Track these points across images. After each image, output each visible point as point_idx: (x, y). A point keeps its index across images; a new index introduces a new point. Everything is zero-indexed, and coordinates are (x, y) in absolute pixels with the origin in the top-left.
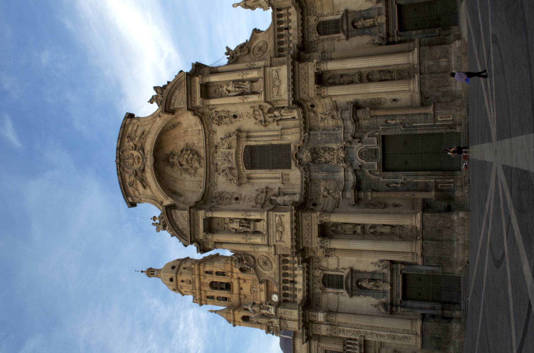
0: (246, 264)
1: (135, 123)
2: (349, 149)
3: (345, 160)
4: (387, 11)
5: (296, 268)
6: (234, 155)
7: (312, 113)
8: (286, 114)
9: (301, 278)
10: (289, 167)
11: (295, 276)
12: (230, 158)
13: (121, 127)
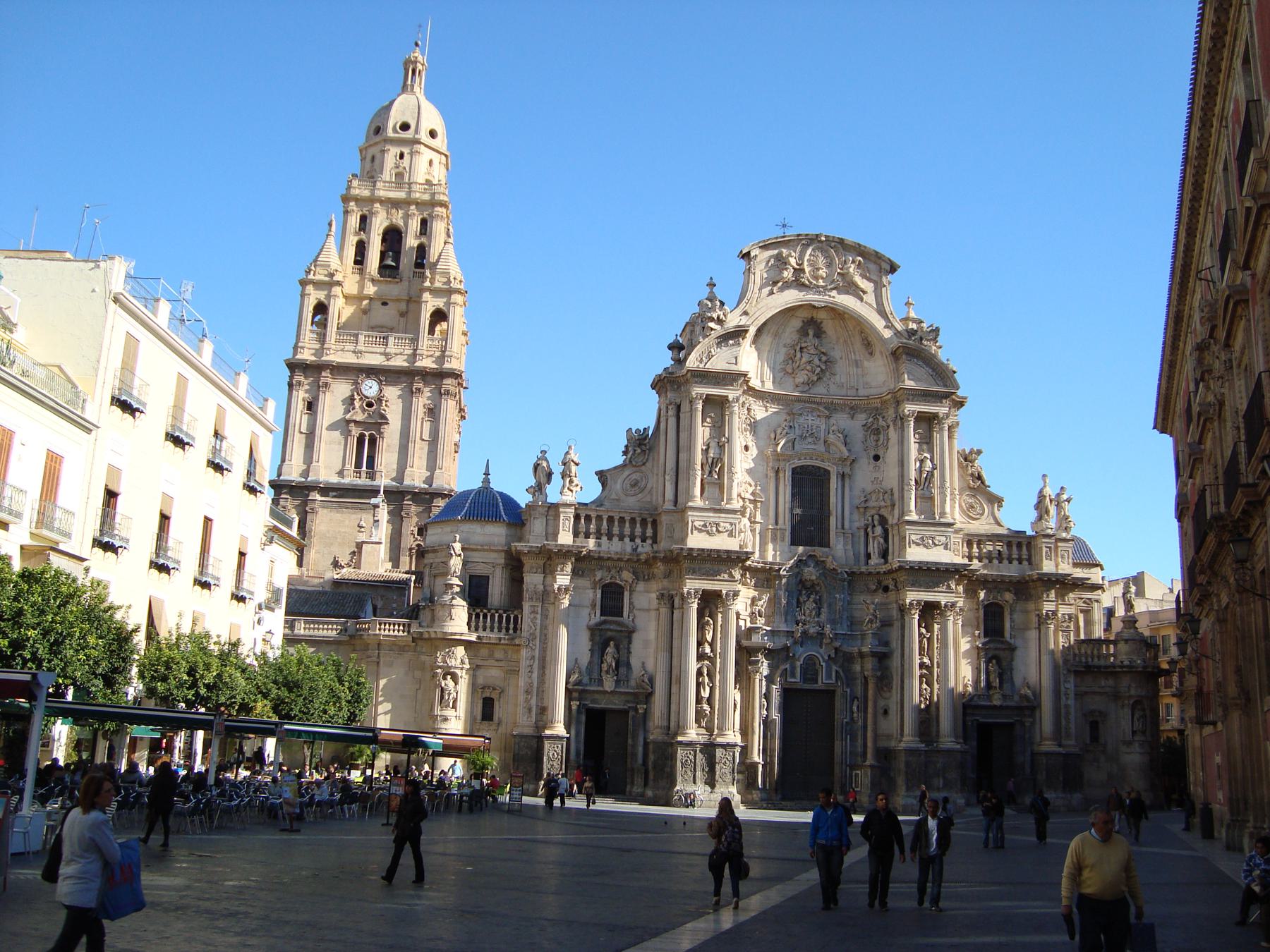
0: (635, 451)
1: (881, 277)
2: (818, 641)
3: (804, 633)
4: (1007, 707)
5: (634, 541)
6: (813, 447)
7: (875, 587)
8: (876, 545)
9: (619, 550)
10: (795, 542)
11: (621, 538)
12: (810, 440)
13: (877, 253)
